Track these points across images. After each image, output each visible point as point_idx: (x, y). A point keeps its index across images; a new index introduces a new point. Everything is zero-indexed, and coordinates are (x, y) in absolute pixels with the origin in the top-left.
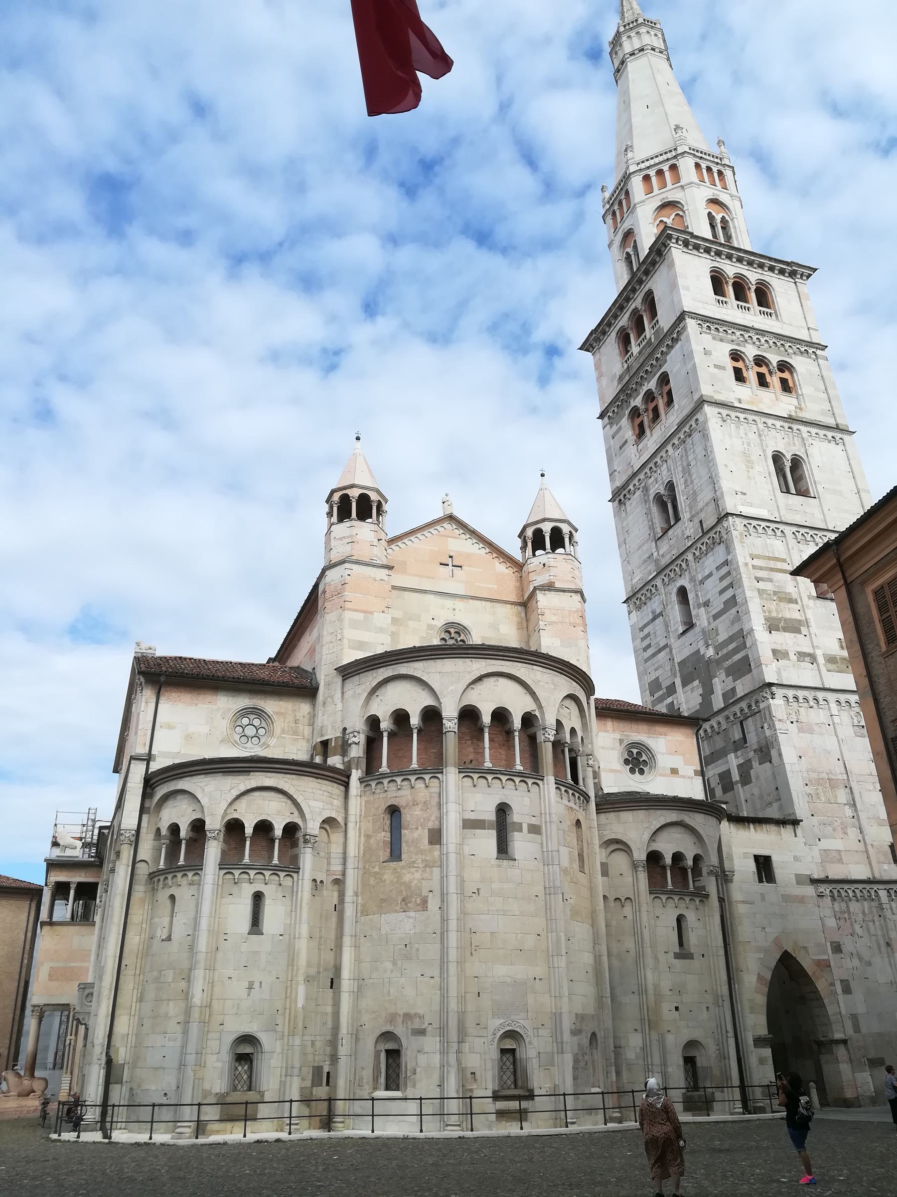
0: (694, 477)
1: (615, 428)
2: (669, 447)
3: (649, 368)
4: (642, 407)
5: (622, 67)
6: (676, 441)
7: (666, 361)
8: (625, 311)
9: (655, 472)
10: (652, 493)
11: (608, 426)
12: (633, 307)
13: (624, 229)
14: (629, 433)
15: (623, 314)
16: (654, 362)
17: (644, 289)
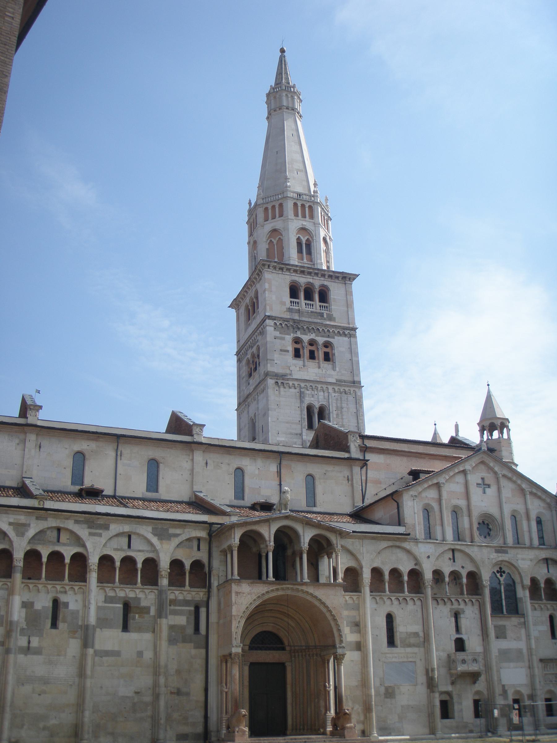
0: (344, 417)
1: (277, 334)
2: (330, 388)
3: (321, 330)
4: (306, 344)
5: (290, 110)
6: (336, 388)
7: (334, 338)
8: (303, 276)
9: (313, 391)
10: (308, 400)
11: (273, 328)
12: (311, 281)
13: (306, 225)
14: (290, 348)
15: (301, 276)
16: (326, 330)
17: (323, 282)
